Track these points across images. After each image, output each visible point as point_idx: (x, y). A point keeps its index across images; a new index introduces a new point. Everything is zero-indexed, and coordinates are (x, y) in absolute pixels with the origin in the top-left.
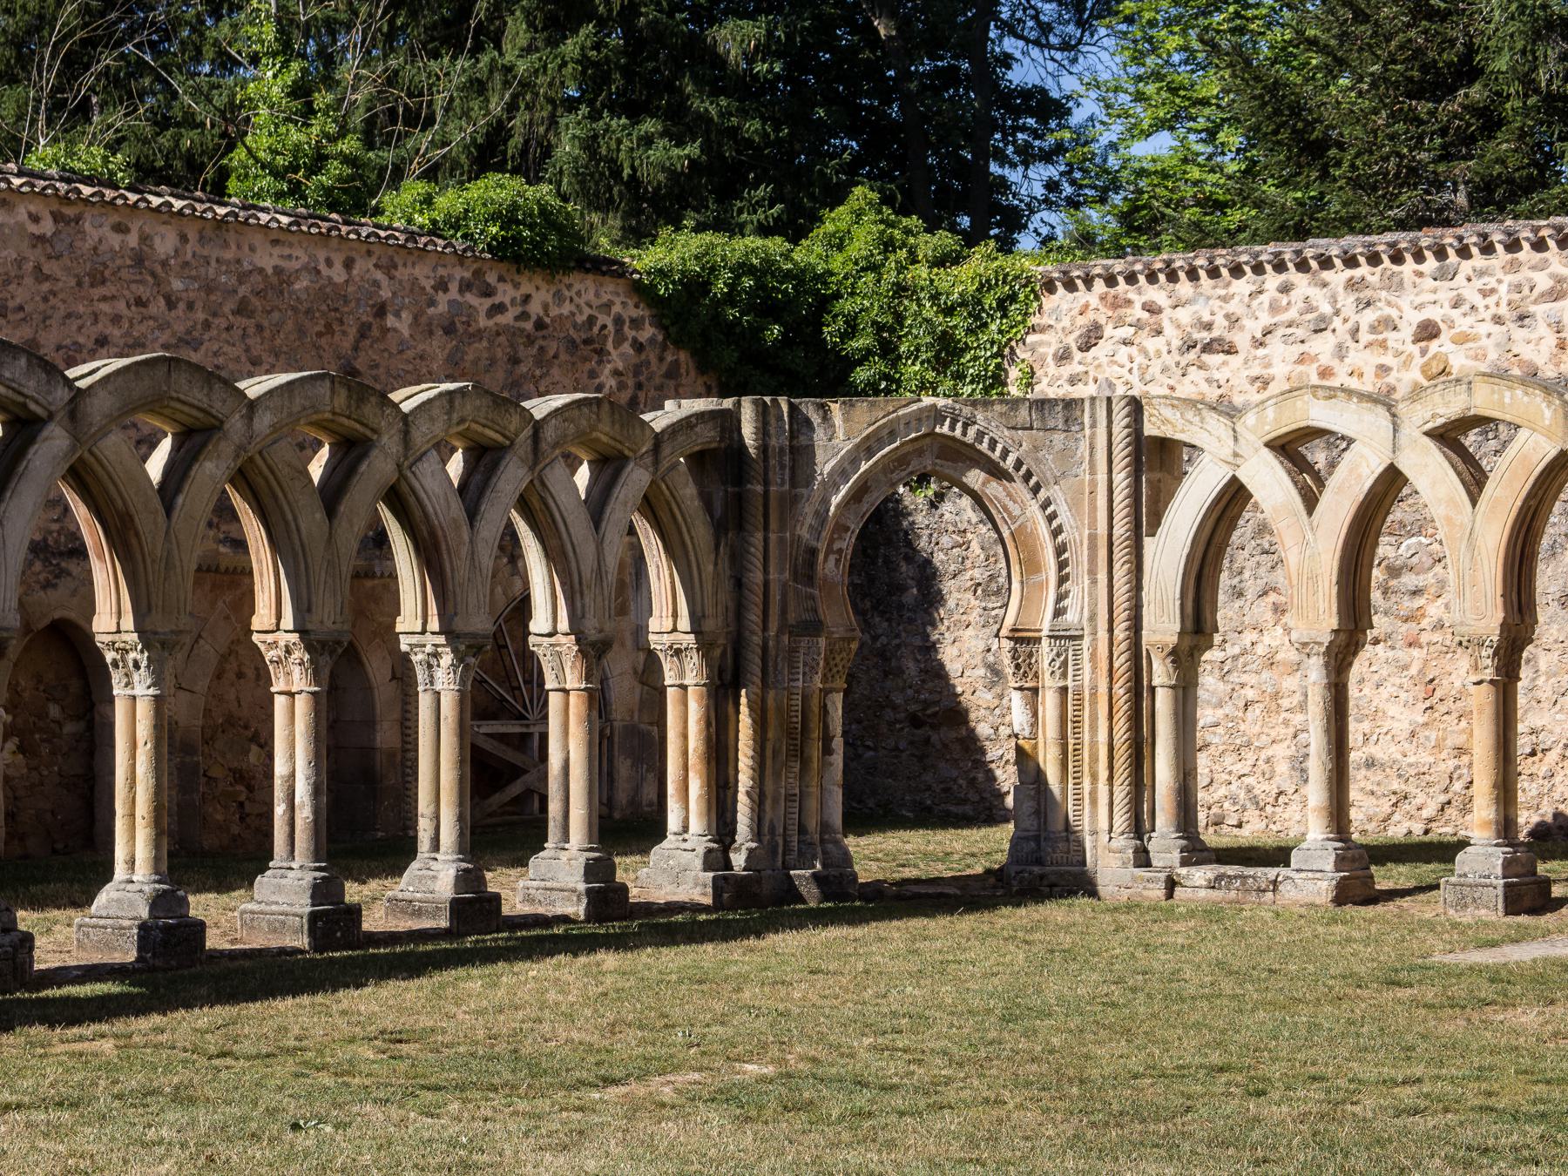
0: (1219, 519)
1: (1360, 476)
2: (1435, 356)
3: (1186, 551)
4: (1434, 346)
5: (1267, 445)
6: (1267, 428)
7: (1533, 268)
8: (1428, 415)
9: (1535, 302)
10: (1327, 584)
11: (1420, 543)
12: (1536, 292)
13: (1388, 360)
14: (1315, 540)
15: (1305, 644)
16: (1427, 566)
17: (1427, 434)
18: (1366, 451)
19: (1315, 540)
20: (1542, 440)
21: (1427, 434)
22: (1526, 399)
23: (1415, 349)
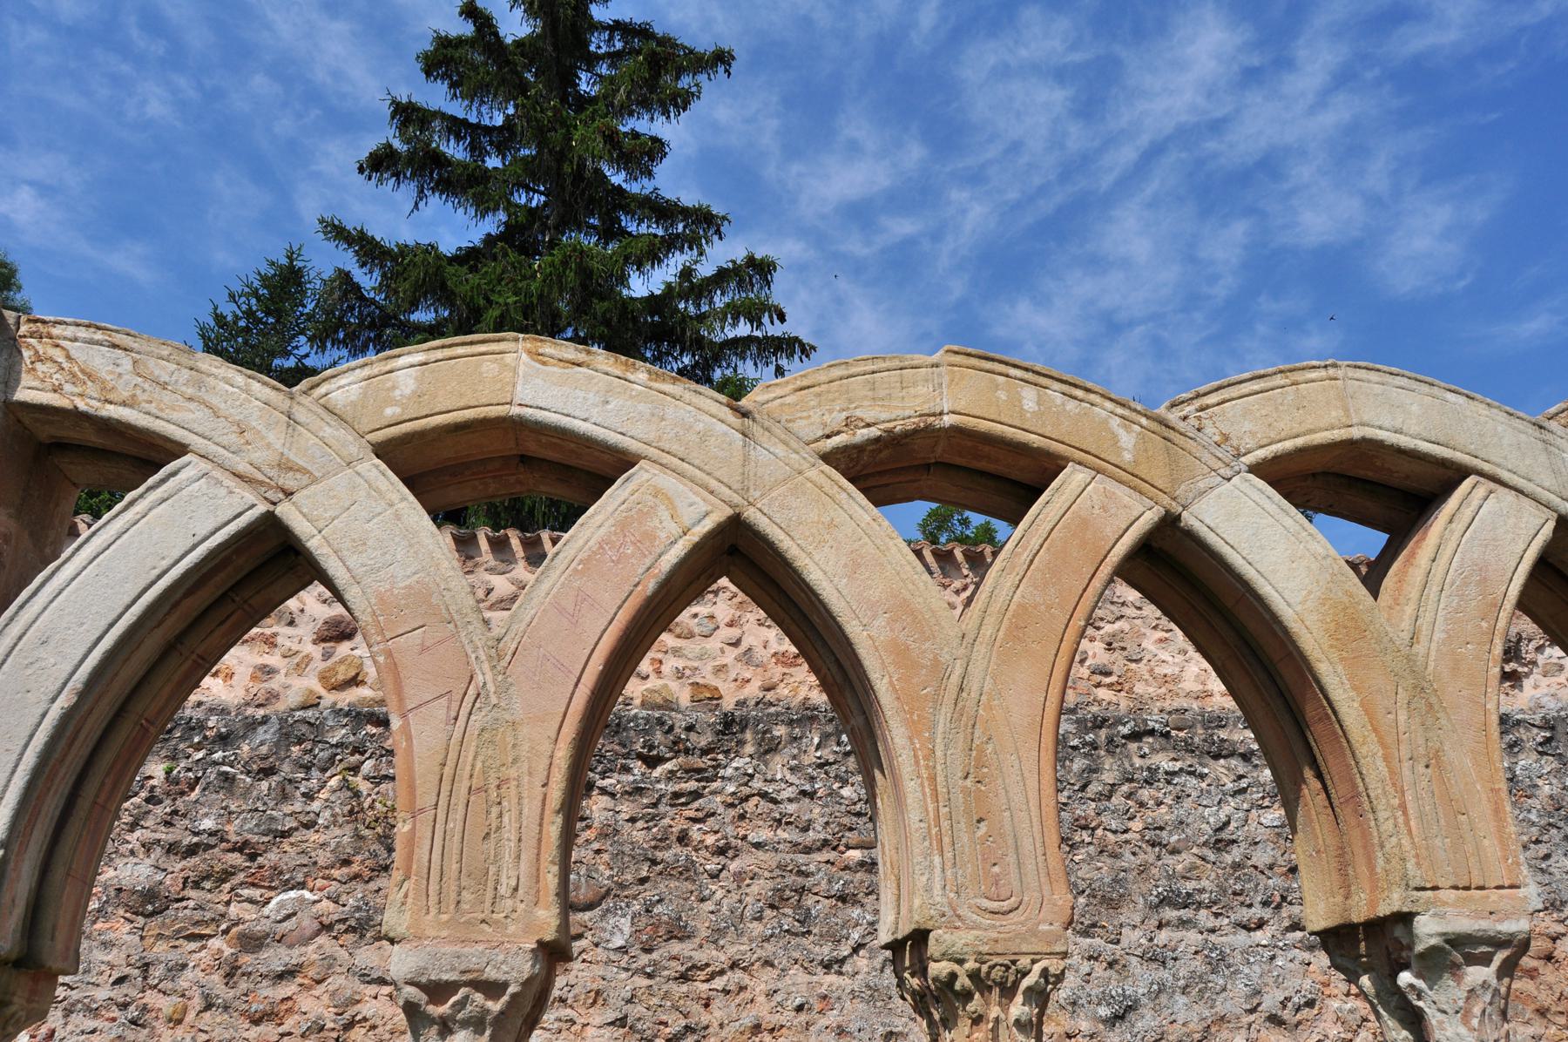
0: (169, 649)
1: (650, 536)
2: (342, 662)
3: (65, 701)
4: (344, 648)
5: (384, 451)
6: (391, 412)
7: (490, 570)
8: (836, 419)
9: (491, 608)
10: (531, 810)
11: (302, 900)
12: (493, 597)
13: (274, 660)
14: (503, 690)
15: (438, 991)
16: (308, 933)
17: (827, 458)
18: (668, 482)
19: (503, 690)
20: (1122, 492)
21: (827, 458)
22: (1071, 405)
23: (316, 651)
